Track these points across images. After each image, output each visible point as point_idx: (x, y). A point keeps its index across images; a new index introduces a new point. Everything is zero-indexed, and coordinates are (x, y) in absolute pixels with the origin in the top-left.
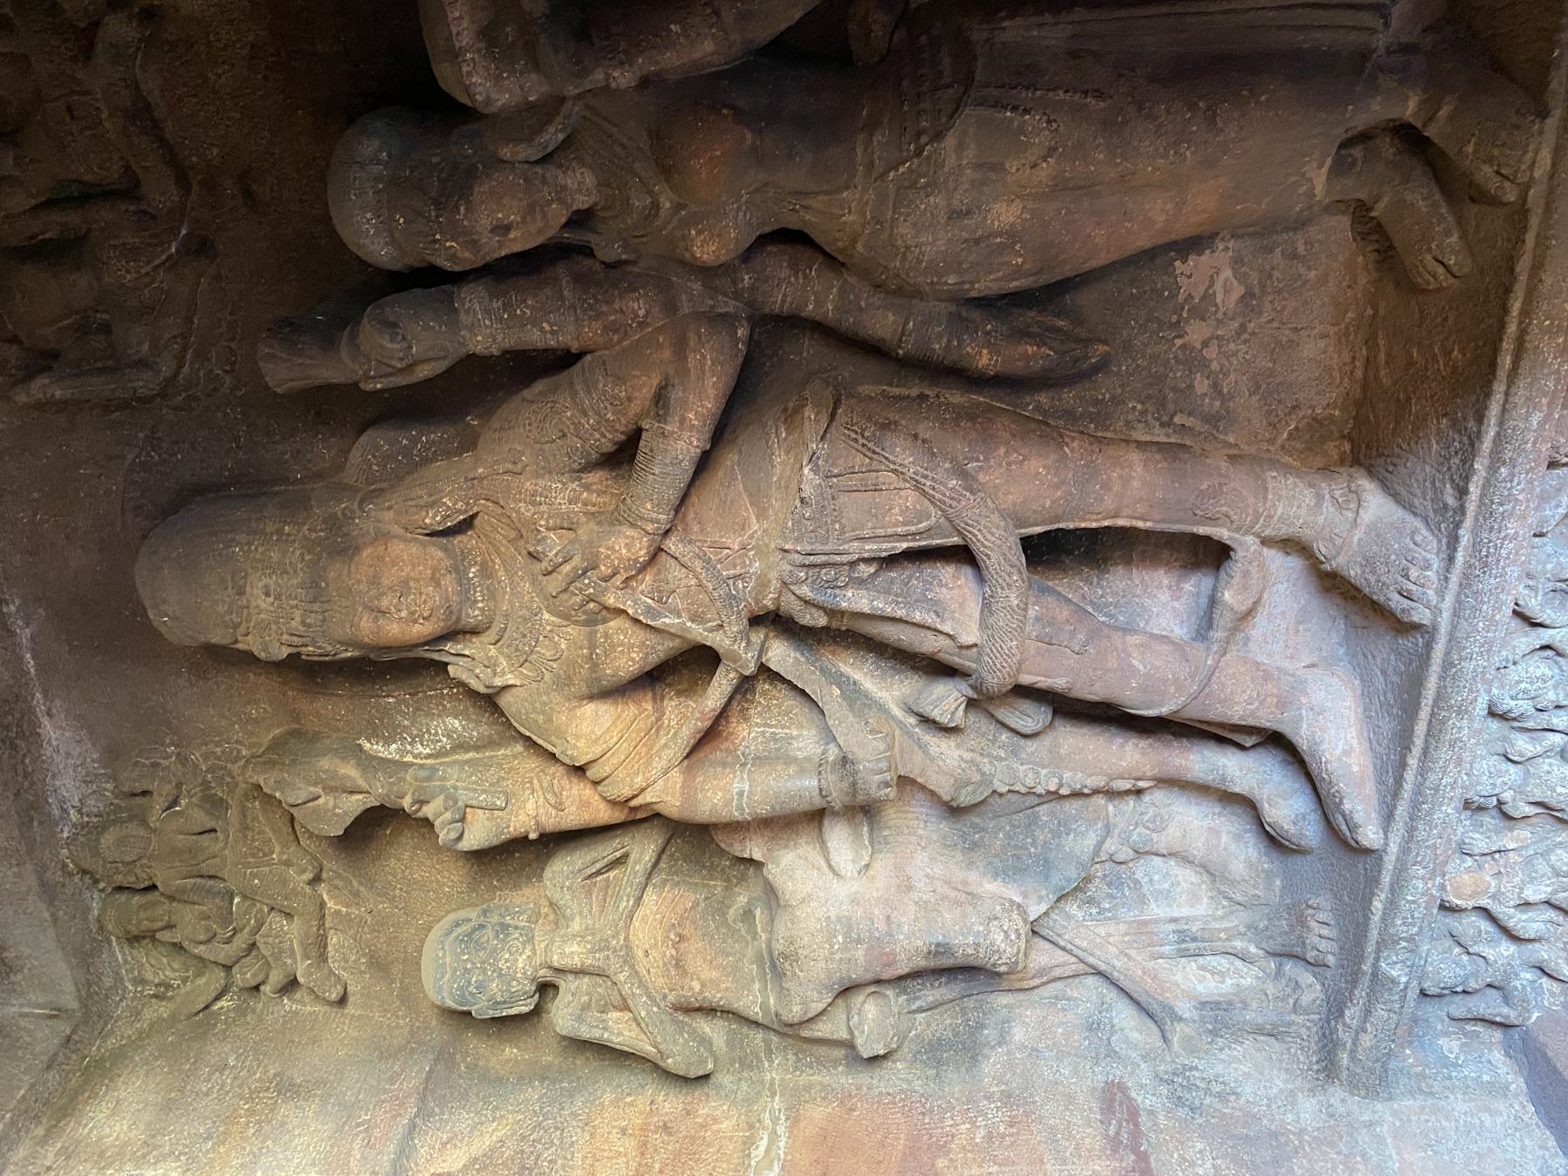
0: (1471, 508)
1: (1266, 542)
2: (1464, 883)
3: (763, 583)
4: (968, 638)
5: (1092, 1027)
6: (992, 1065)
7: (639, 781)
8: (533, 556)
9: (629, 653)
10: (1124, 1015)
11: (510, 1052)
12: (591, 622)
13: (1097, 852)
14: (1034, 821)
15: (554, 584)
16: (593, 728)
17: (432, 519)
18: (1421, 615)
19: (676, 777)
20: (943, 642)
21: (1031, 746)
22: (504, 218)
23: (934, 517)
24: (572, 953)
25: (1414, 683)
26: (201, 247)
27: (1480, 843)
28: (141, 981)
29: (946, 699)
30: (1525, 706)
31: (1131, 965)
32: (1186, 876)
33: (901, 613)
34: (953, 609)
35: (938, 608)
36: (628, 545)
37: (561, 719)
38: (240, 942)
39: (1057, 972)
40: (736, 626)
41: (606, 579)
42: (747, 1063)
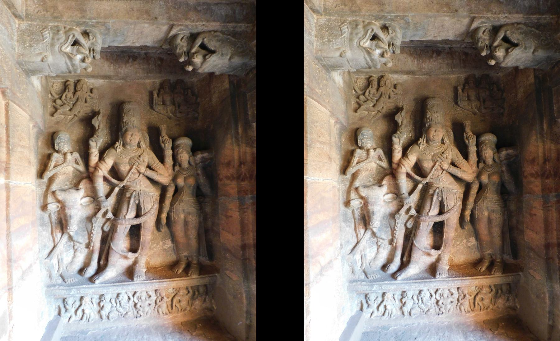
0: (455, 279)
3: (438, 184)
5: (348, 242)
6: (343, 224)
7: (406, 166)
10: (351, 247)
11: (343, 140)
15: (439, 155)
16: (412, 159)
18: (437, 276)
19: (405, 171)
20: (428, 211)
25: (426, 278)
28: (357, 79)
31: (360, 247)
33: (433, 204)
35: (434, 209)
37: (414, 154)
38: (369, 98)
39: (359, 234)
41: (441, 163)
42: (343, 181)
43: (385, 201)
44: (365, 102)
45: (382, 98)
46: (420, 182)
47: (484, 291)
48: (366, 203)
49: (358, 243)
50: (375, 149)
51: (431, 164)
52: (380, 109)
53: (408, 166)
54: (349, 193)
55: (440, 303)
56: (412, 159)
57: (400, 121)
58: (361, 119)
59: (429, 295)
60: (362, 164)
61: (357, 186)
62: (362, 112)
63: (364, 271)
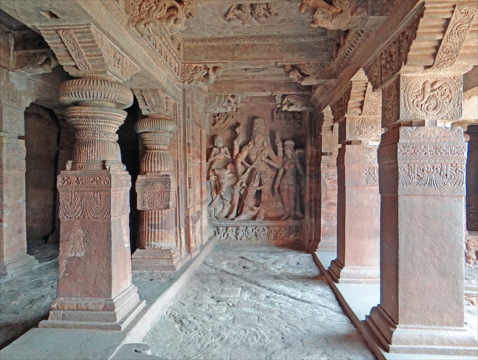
1: (259, 210)
2: (230, 228)
4: (254, 186)
8: (262, 151)
9: (253, 158)
10: (209, 203)
12: (256, 155)
13: (226, 200)
14: (229, 193)
16: (245, 154)
17: (264, 143)
18: (256, 220)
19: (240, 161)
21: (238, 193)
22: (289, 152)
23: (265, 182)
24: (222, 150)
26: (284, 127)
27: (233, 230)
29: (244, 185)
30: (248, 229)
31: (214, 203)
32: (221, 210)
34: (256, 184)
36: (263, 159)
40: (255, 166)
43: (228, 178)
44: (219, 120)
45: (228, 118)
46: (249, 167)
47: (282, 229)
48: (218, 177)
49: (213, 201)
50: (223, 147)
51: (255, 157)
52: (227, 124)
53: (242, 158)
54: (208, 172)
55: (257, 234)
56: (245, 154)
57: (238, 132)
58: (216, 130)
59: (251, 230)
60: (217, 156)
61: (213, 168)
62: (217, 125)
63: (216, 217)
